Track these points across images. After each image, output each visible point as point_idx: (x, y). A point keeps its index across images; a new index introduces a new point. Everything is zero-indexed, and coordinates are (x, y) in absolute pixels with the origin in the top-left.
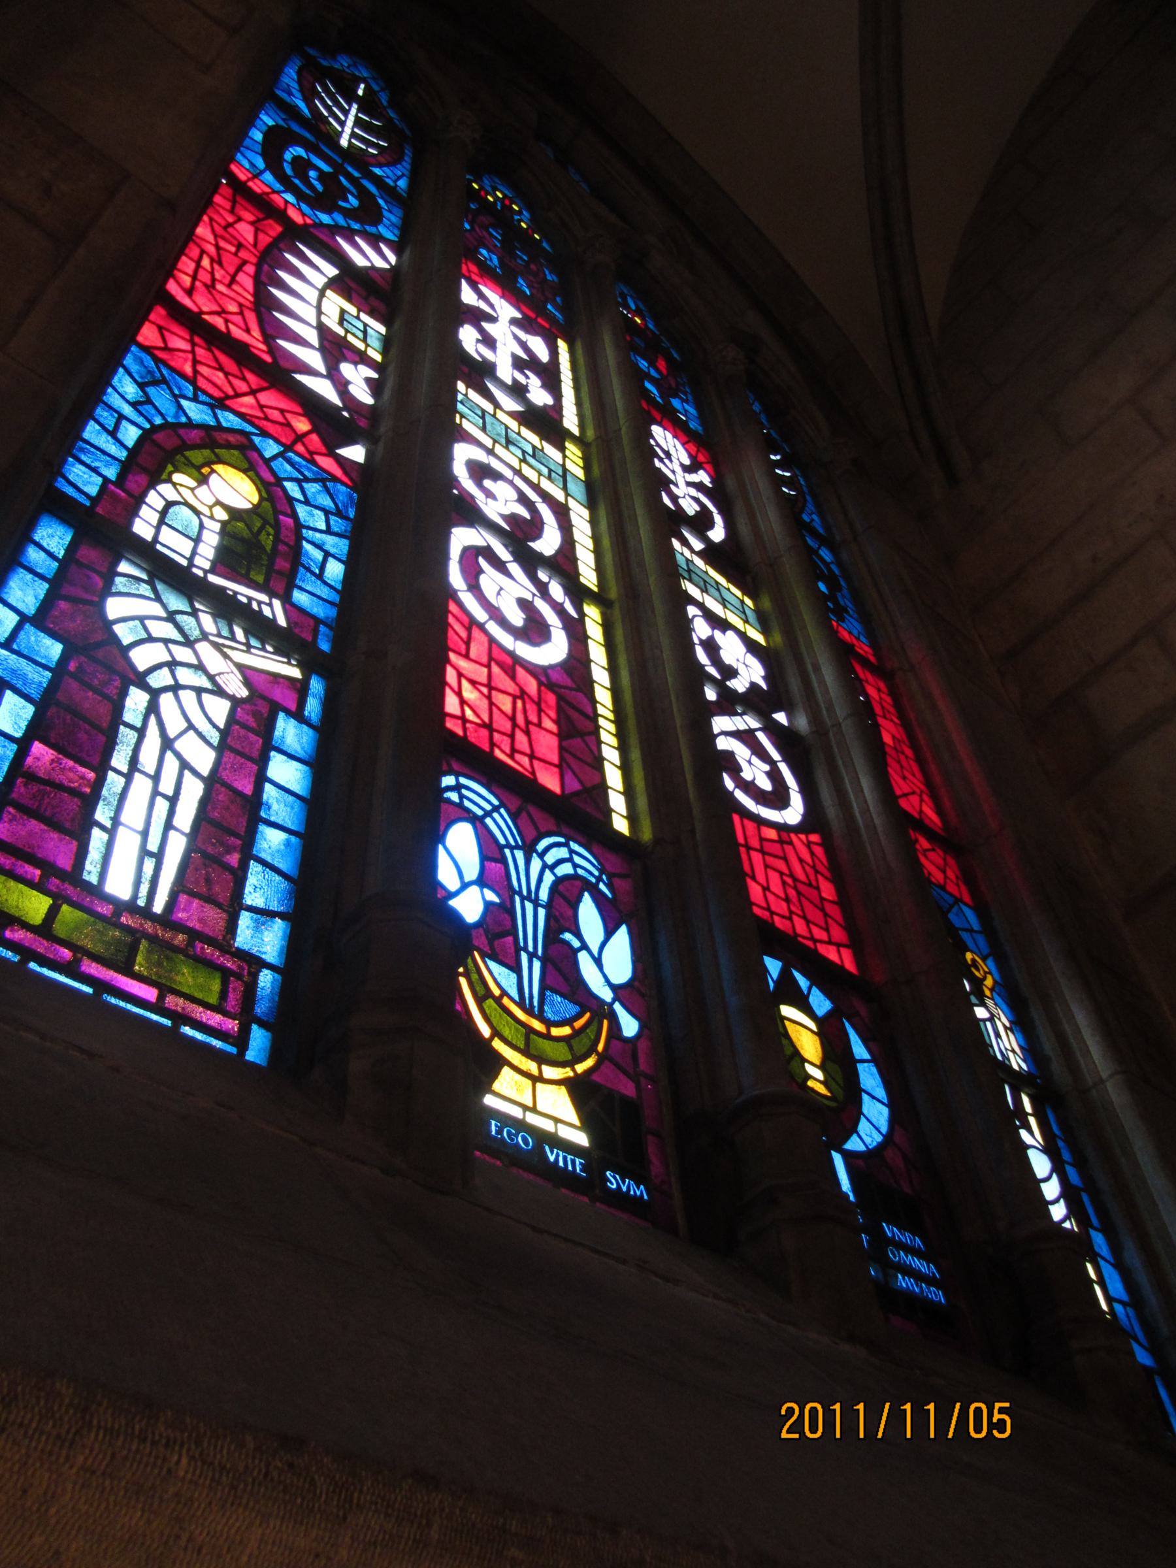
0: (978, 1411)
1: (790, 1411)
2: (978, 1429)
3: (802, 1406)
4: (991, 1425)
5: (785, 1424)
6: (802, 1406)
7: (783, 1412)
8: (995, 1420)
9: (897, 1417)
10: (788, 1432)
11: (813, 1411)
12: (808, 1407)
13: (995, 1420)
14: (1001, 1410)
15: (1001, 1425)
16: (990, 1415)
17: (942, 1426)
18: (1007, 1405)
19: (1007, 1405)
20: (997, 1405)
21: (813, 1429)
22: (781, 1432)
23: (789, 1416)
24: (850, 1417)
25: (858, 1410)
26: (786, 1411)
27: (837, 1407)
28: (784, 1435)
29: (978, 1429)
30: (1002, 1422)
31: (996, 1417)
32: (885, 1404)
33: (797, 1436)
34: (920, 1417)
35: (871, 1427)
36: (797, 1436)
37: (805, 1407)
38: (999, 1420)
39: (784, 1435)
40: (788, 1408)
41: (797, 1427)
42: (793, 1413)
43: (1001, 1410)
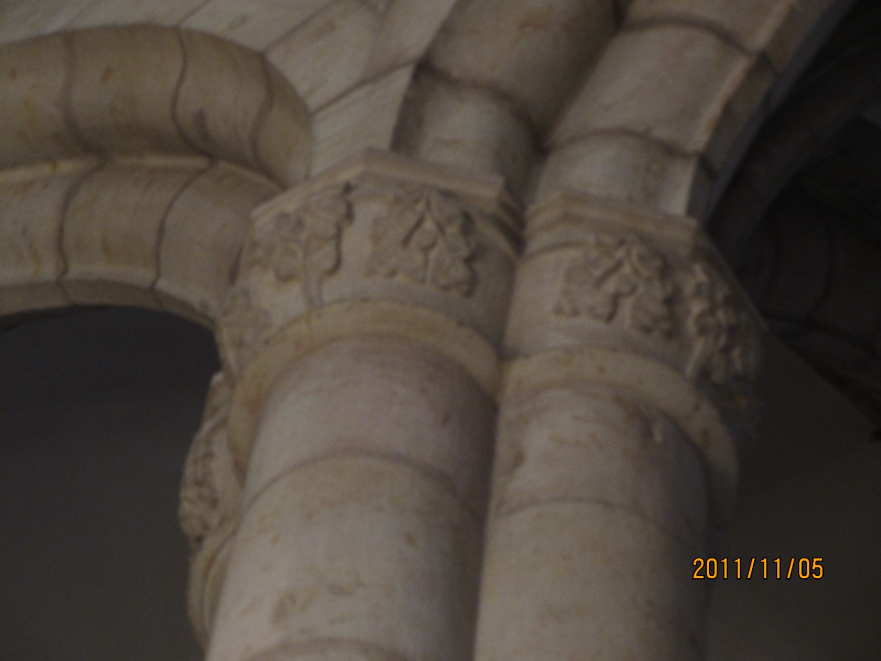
0: (804, 563)
1: (699, 563)
2: (804, 574)
3: (705, 561)
5: (696, 570)
6: (705, 561)
7: (695, 564)
8: (814, 568)
9: (759, 566)
10: (697, 575)
11: (712, 563)
13: (814, 568)
14: (817, 563)
15: (817, 571)
16: (811, 566)
18: (821, 559)
19: (821, 559)
20: (815, 560)
21: (712, 574)
22: (693, 575)
23: (698, 565)
24: (732, 566)
25: (737, 563)
26: (697, 563)
27: (725, 561)
28: (695, 577)
29: (804, 574)
32: (752, 559)
33: (702, 577)
34: (772, 566)
35: (784, 571)
36: (702, 577)
37: (707, 561)
38: (816, 568)
39: (695, 577)
40: (697, 561)
41: (703, 572)
42: (701, 564)
43: (817, 563)
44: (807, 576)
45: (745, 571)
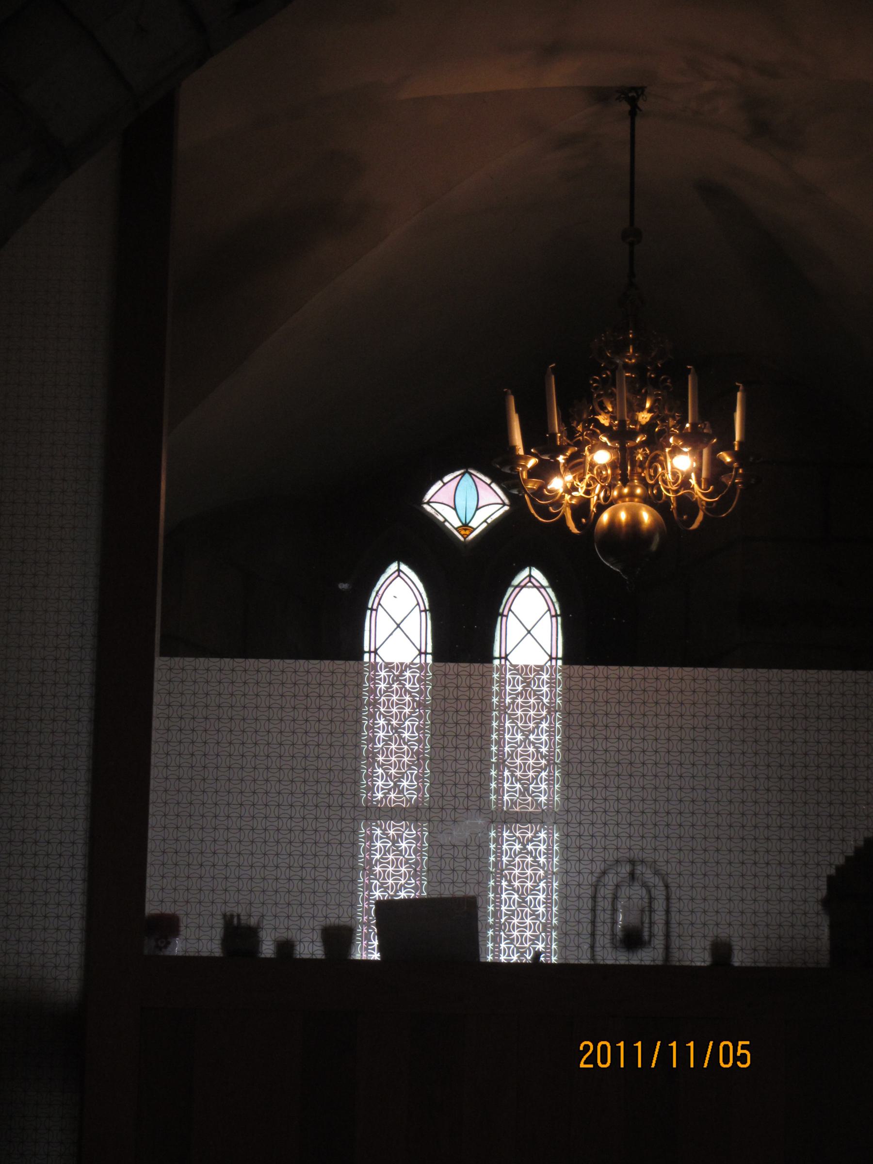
0: (726, 1048)
1: (587, 1048)
2: (726, 1061)
4: (736, 1058)
5: (583, 1057)
7: (581, 1048)
8: (738, 1054)
9: (666, 1052)
10: (585, 1063)
11: (604, 1048)
12: (600, 1044)
13: (738, 1054)
14: (743, 1047)
15: (743, 1058)
16: (735, 1050)
17: (699, 1058)
18: (748, 1043)
19: (748, 1043)
20: (740, 1043)
21: (604, 1061)
22: (580, 1063)
24: (631, 1053)
26: (584, 1047)
27: (622, 1044)
28: (582, 1065)
29: (726, 1061)
30: (744, 1056)
31: (740, 1052)
33: (591, 1066)
34: (683, 1052)
36: (591, 1066)
37: (597, 1045)
38: (741, 1054)
39: (582, 1065)
40: (585, 1046)
41: (592, 1059)
43: (743, 1047)
44: (730, 1065)
45: (647, 1058)
